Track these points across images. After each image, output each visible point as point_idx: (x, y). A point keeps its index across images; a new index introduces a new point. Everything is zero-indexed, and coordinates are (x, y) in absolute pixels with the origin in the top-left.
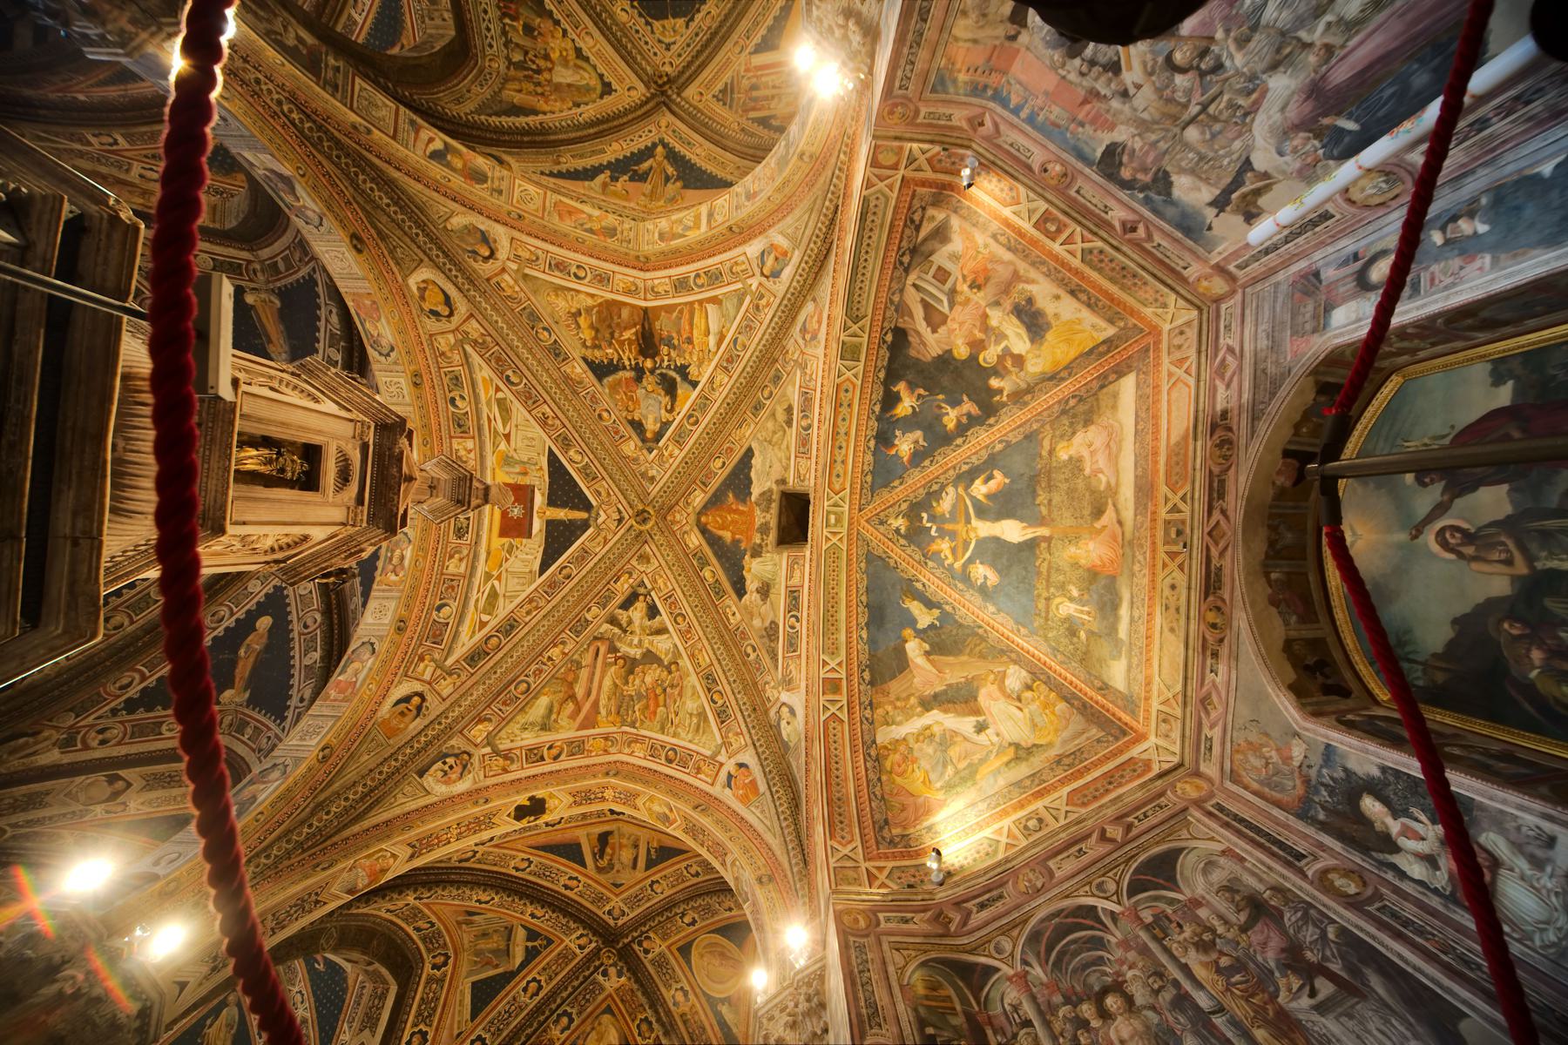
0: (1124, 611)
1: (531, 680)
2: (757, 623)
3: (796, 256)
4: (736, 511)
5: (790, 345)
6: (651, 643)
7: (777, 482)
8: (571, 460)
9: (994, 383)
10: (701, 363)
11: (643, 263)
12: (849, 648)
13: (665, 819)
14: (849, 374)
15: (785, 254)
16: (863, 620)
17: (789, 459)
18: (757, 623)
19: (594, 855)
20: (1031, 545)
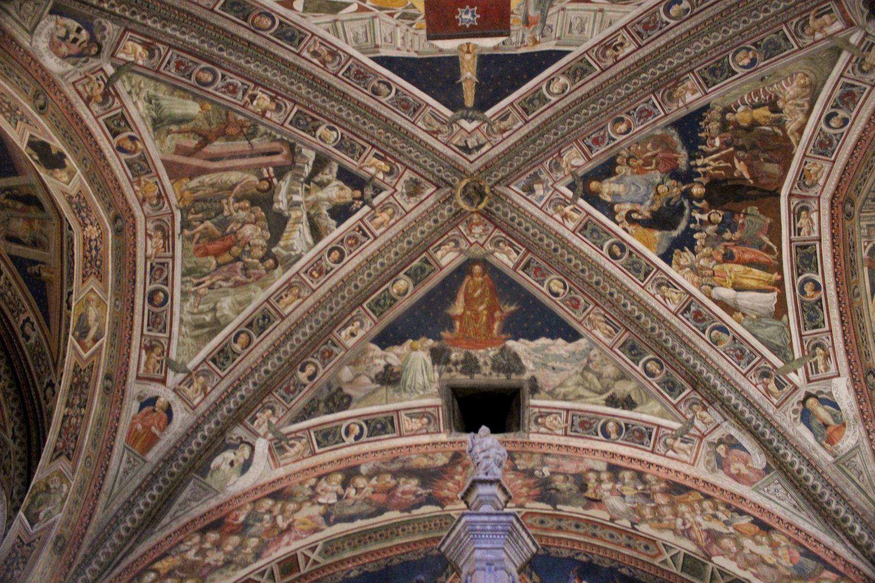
1: (219, 83)
2: (347, 373)
3: (823, 456)
4: (491, 319)
5: (713, 415)
6: (298, 221)
7: (533, 380)
8: (550, 80)
10: (696, 270)
11: (842, 205)
12: (335, 564)
13: (83, 330)
14: (667, 556)
15: (831, 441)
16: (370, 568)
17: (565, 398)
18: (347, 373)
19: (9, 189)
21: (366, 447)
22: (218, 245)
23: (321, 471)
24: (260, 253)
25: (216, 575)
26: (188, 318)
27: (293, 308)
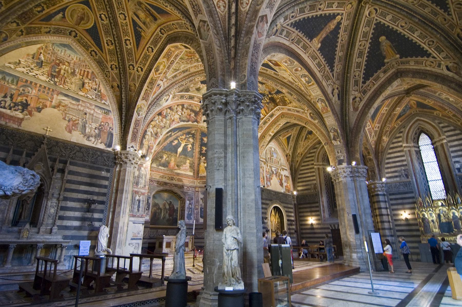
0: (163, 168)
2: (192, 85)
9: (204, 158)
13: (157, 70)
20: (176, 153)
21: (187, 101)
22: (191, 55)
23: (178, 104)
24: (196, 59)
25: (163, 130)
26: (174, 68)
27: (192, 70)
